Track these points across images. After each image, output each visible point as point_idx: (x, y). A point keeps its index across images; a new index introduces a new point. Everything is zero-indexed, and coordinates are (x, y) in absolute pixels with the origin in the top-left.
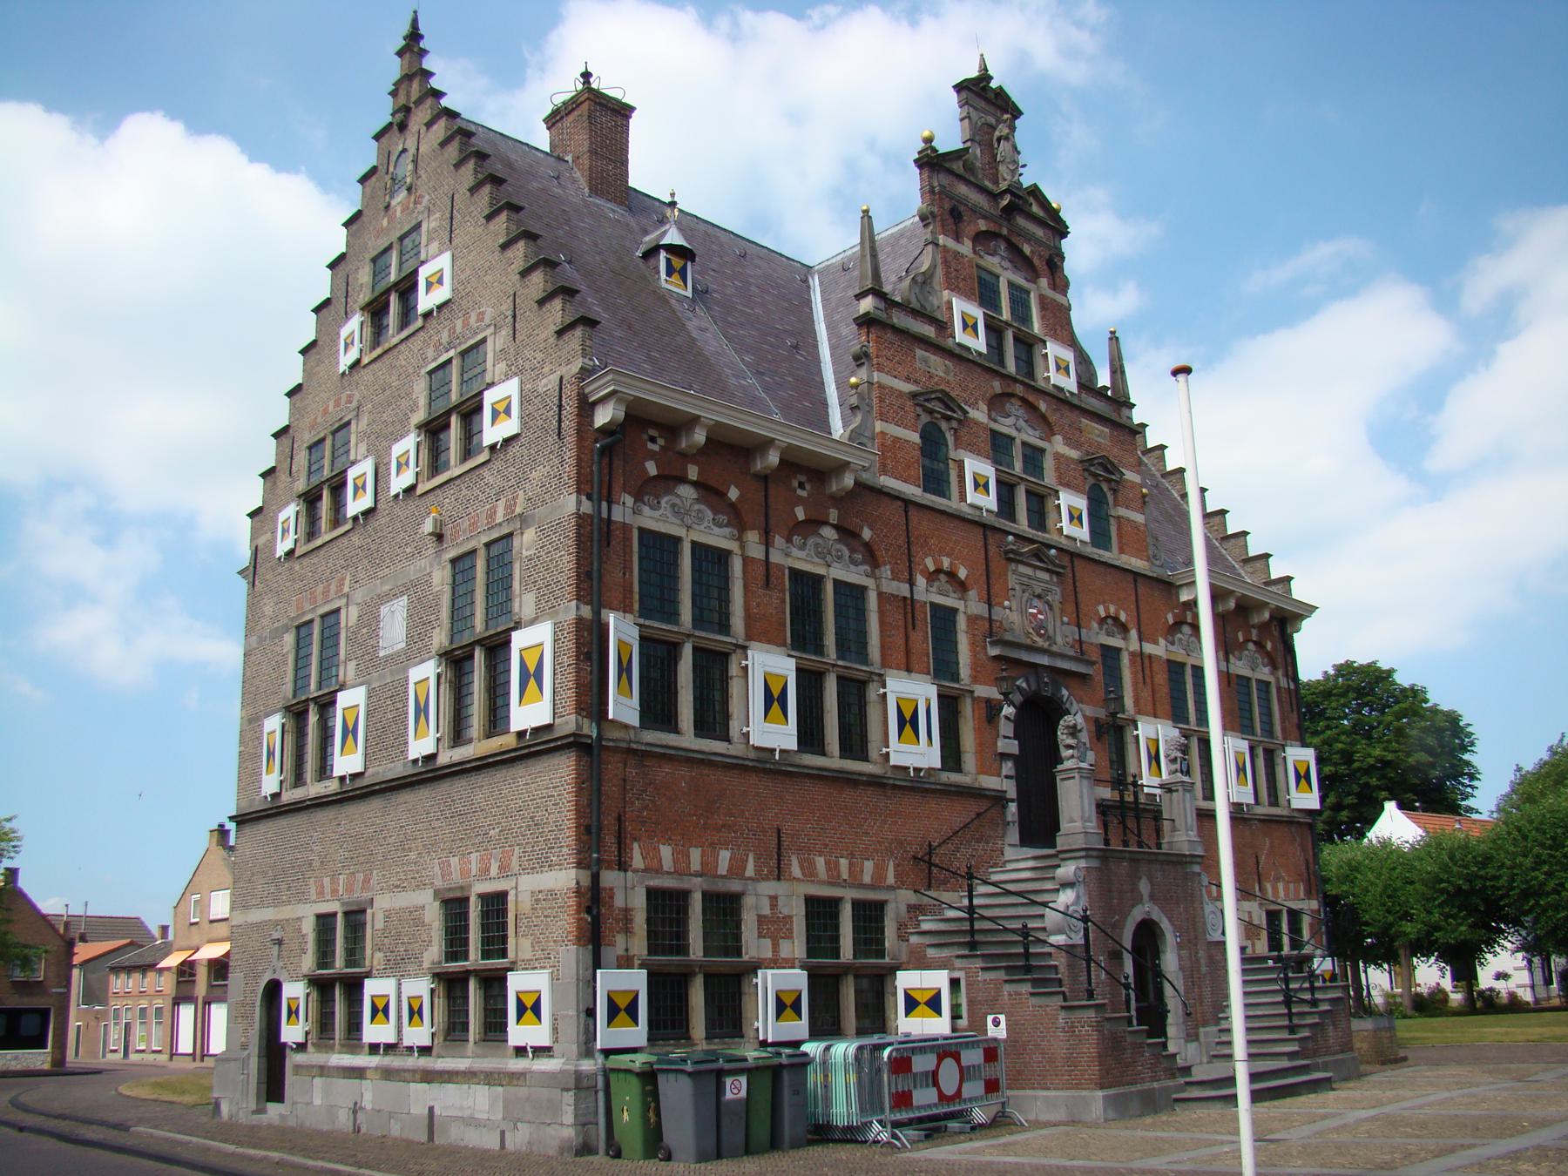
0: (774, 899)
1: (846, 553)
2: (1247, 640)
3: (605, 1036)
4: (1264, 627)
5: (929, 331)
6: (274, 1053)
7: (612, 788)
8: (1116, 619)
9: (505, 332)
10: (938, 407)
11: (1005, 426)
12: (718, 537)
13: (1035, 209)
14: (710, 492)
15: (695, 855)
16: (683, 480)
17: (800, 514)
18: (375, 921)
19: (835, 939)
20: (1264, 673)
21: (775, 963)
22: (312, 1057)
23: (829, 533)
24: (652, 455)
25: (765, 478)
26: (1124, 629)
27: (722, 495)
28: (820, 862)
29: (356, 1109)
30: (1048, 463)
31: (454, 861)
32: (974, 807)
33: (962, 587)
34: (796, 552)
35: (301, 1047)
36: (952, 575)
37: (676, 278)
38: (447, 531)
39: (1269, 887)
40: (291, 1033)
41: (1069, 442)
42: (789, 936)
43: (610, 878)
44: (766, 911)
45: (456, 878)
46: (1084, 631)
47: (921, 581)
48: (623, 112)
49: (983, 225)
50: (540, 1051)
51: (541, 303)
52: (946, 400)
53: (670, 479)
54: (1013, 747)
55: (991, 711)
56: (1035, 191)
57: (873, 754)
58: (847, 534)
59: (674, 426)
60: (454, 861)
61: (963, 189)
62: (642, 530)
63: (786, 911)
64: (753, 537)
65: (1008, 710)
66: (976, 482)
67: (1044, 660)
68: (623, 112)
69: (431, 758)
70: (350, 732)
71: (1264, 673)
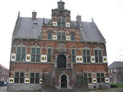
0: (27, 73)
2: (96, 46)
5: (50, 25)
7: (12, 66)
8: (74, 47)
10: (50, 32)
11: (60, 32)
12: (25, 46)
14: (24, 43)
15: (20, 70)
16: (21, 43)
17: (33, 43)
19: (34, 76)
21: (27, 78)
26: (75, 48)
30: (66, 34)
32: (51, 65)
33: (52, 47)
36: (51, 46)
39: (98, 71)
41: (68, 32)
43: (11, 72)
44: (26, 74)
46: (68, 49)
47: (46, 47)
48: (36, 13)
49: (58, 14)
52: (51, 31)
55: (54, 57)
58: (38, 44)
61: (56, 12)
64: (28, 46)
66: (55, 37)
67: (61, 52)
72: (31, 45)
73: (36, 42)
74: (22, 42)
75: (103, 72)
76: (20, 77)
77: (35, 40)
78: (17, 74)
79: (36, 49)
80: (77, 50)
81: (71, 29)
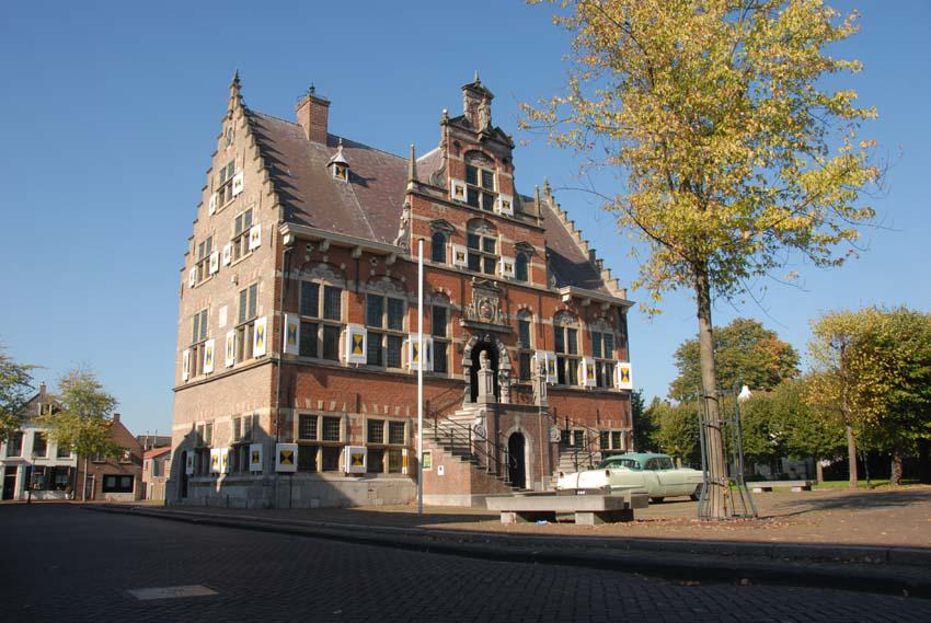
1: (394, 287)
3: (279, 467)
4: (607, 311)
5: (440, 194)
6: (184, 478)
9: (258, 206)
13: (499, 138)
14: (333, 266)
16: (322, 262)
17: (373, 272)
18: (215, 428)
20: (609, 331)
22: (195, 479)
23: (387, 279)
24: (308, 253)
25: (357, 260)
27: (338, 267)
28: (376, 406)
29: (207, 497)
31: (238, 405)
34: (371, 287)
35: (192, 476)
36: (444, 294)
37: (340, 175)
38: (240, 281)
40: (189, 471)
42: (361, 433)
45: (239, 412)
49: (470, 147)
50: (259, 473)
51: (269, 195)
53: (315, 262)
54: (470, 363)
56: (498, 130)
57: (403, 366)
58: (394, 279)
59: (318, 242)
60: (238, 405)
62: (303, 282)
63: (358, 425)
65: (468, 347)
68: (326, 104)
69: (232, 366)
70: (209, 356)
71: (609, 331)
72: (370, 279)
73: (389, 267)
74: (325, 259)
75: (619, 427)
76: (319, 438)
77: (383, 256)
78: (307, 422)
79: (386, 300)
80: (540, 324)
81: (516, 228)
